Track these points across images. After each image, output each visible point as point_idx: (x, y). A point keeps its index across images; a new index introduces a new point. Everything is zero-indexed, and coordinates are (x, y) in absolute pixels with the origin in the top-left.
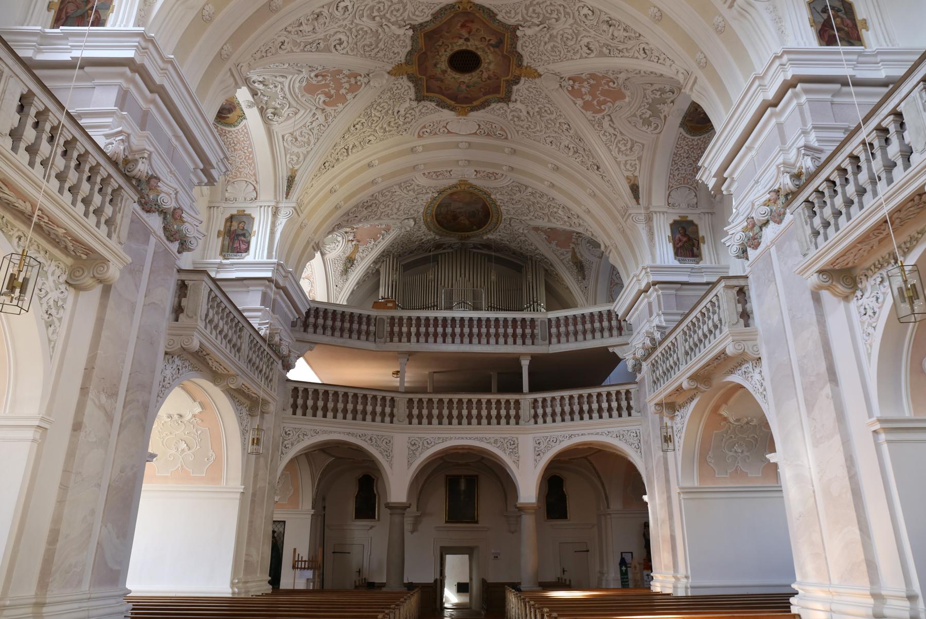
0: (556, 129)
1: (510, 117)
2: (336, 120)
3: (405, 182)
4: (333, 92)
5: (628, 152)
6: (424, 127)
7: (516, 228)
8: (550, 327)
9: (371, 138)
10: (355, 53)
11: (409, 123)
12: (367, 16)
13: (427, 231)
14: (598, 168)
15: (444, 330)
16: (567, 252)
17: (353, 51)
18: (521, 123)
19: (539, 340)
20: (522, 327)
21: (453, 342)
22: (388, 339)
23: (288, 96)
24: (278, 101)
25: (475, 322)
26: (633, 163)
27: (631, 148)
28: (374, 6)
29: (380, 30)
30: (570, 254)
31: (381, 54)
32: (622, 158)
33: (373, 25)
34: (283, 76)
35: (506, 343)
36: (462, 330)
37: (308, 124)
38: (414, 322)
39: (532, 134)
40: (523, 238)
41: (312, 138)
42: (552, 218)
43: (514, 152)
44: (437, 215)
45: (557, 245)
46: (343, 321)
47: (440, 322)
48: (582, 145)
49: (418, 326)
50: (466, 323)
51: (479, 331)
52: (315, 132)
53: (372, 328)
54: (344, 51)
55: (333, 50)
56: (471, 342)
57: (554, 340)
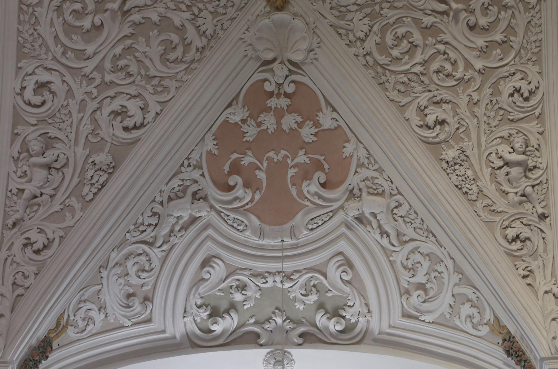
2: (390, 171)
4: (302, 158)
10: (172, 84)
12: (88, 41)
17: (166, 89)
23: (289, 266)
24: (297, 293)
28: (65, 22)
29: (136, 17)
31: (208, 23)
33: (115, 30)
34: (206, 263)
37: (385, 242)
52: (409, 232)
54: (154, 108)
55: (135, 134)
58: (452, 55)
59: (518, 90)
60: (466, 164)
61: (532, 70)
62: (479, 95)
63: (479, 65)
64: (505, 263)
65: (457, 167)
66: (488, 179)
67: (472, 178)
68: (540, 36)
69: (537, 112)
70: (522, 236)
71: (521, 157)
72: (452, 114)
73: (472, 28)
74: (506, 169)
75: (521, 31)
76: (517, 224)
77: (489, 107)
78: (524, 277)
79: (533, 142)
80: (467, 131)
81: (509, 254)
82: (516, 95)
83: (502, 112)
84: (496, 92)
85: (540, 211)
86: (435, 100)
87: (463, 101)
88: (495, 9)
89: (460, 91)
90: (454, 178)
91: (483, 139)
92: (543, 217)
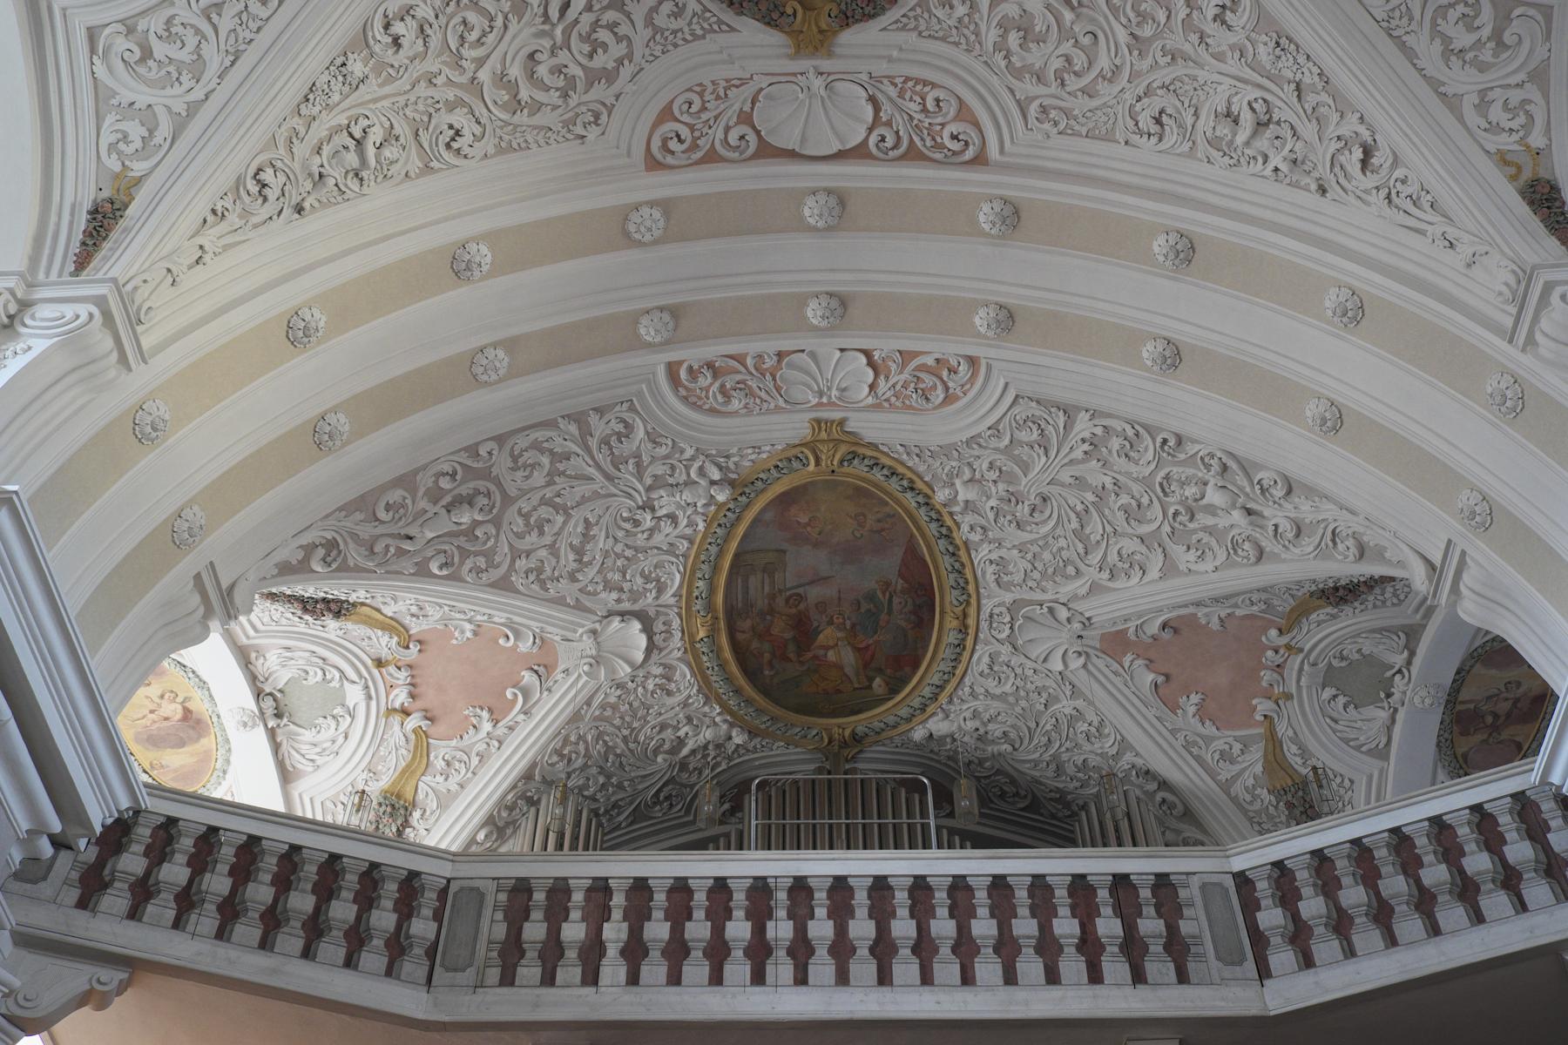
0: (1176, 40)
1: (991, 36)
3: (600, 411)
5: (1487, 55)
6: (666, 114)
7: (1037, 651)
8: (1250, 906)
9: (459, 118)
11: (610, 76)
13: (697, 702)
14: (1367, 152)
15: (759, 930)
16: (1246, 745)
18: (1035, 56)
19: (1207, 960)
20: (1119, 911)
21: (801, 979)
22: (494, 974)
25: (901, 897)
26: (1515, 96)
27: (1497, 36)
30: (1256, 754)
32: (1462, 80)
35: (1052, 977)
36: (841, 931)
38: (618, 900)
39: (1080, 104)
40: (1065, 706)
41: (209, 50)
42: (1177, 550)
43: (1013, 216)
44: (731, 612)
45: (1202, 714)
46: (283, 883)
47: (739, 898)
48: (1287, 69)
49: (638, 914)
50: (861, 898)
51: (922, 930)
53: (422, 927)
56: (884, 978)
57: (1282, 957)
58: (491, 39)
59: (458, 133)
60: (347, 88)
61: (488, 144)
62: (445, 84)
63: (484, 75)
64: (225, 179)
65: (340, 78)
66: (333, 123)
67: (330, 101)
68: (533, 146)
69: (435, 164)
70: (267, 191)
71: (372, 162)
72: (411, 54)
73: (531, 56)
74: (351, 144)
75: (538, 120)
76: (282, 178)
77: (430, 101)
78: (214, 212)
79: (394, 169)
80: (391, 79)
81: (239, 182)
82: (452, 132)
83: (426, 119)
84: (451, 107)
85: (306, 205)
86: (426, 27)
87: (432, 65)
88: (561, 83)
89: (444, 58)
90: (325, 77)
91: (386, 103)
92: (299, 209)
